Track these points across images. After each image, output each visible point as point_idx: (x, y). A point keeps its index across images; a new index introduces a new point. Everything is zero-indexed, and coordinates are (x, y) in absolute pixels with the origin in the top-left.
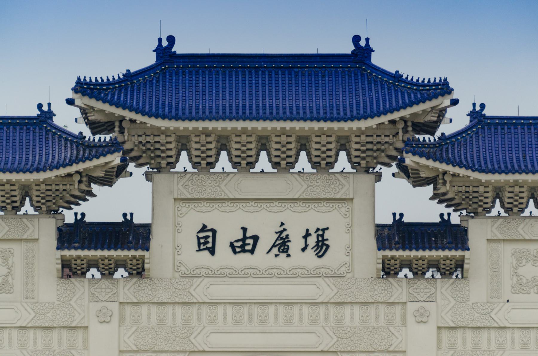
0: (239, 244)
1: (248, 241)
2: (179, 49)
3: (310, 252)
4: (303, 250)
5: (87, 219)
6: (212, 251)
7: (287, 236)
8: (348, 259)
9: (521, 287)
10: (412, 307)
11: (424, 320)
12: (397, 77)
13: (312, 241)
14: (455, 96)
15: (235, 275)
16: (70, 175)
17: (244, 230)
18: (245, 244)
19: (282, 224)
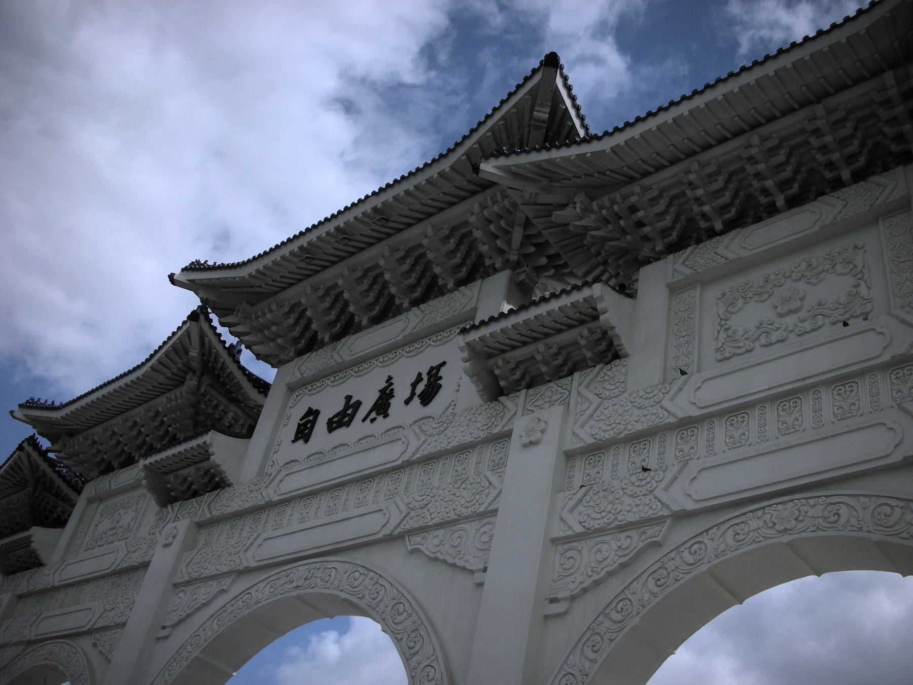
0: (336, 419)
1: (349, 412)
3: (416, 401)
4: (407, 402)
7: (393, 389)
10: (520, 425)
11: (533, 439)
13: (420, 388)
15: (320, 459)
19: (390, 378)
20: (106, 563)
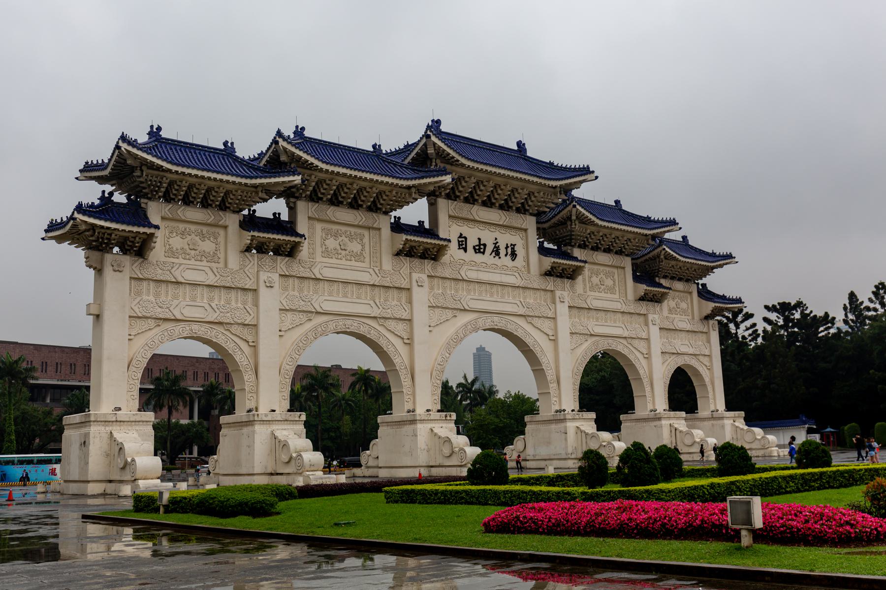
2: (443, 128)
3: (509, 257)
5: (402, 221)
6: (465, 250)
8: (524, 264)
9: (592, 288)
12: (551, 164)
13: (509, 250)
14: (595, 174)
16: (409, 188)
17: (479, 239)
18: (480, 248)
20: (365, 277)
